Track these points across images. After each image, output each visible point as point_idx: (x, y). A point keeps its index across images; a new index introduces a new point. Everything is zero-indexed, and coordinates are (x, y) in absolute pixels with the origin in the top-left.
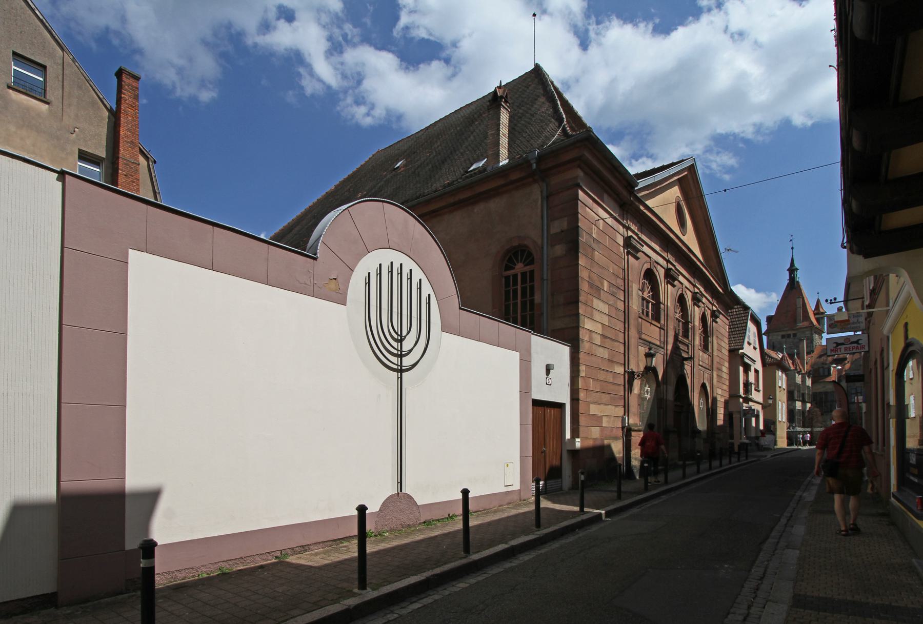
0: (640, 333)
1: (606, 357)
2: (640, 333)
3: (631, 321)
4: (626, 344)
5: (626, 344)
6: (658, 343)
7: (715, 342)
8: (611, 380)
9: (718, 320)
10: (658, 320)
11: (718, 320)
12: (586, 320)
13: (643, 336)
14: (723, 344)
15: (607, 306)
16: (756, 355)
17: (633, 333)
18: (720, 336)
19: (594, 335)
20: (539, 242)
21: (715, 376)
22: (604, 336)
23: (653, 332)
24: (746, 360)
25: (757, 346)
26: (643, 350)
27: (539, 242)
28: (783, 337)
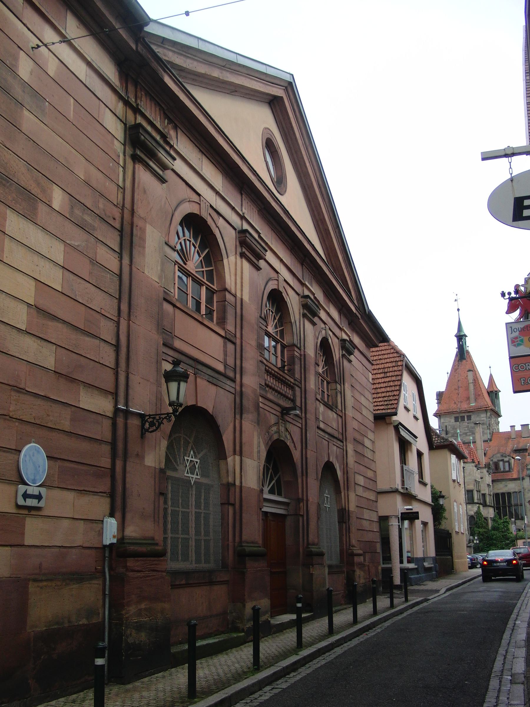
1: (50, 362)
6: (220, 367)
7: (348, 393)
8: (66, 425)
9: (352, 357)
10: (222, 322)
11: (352, 357)
14: (363, 400)
16: (418, 429)
18: (357, 386)
21: (350, 452)
24: (403, 433)
25: (419, 415)
28: (456, 419)
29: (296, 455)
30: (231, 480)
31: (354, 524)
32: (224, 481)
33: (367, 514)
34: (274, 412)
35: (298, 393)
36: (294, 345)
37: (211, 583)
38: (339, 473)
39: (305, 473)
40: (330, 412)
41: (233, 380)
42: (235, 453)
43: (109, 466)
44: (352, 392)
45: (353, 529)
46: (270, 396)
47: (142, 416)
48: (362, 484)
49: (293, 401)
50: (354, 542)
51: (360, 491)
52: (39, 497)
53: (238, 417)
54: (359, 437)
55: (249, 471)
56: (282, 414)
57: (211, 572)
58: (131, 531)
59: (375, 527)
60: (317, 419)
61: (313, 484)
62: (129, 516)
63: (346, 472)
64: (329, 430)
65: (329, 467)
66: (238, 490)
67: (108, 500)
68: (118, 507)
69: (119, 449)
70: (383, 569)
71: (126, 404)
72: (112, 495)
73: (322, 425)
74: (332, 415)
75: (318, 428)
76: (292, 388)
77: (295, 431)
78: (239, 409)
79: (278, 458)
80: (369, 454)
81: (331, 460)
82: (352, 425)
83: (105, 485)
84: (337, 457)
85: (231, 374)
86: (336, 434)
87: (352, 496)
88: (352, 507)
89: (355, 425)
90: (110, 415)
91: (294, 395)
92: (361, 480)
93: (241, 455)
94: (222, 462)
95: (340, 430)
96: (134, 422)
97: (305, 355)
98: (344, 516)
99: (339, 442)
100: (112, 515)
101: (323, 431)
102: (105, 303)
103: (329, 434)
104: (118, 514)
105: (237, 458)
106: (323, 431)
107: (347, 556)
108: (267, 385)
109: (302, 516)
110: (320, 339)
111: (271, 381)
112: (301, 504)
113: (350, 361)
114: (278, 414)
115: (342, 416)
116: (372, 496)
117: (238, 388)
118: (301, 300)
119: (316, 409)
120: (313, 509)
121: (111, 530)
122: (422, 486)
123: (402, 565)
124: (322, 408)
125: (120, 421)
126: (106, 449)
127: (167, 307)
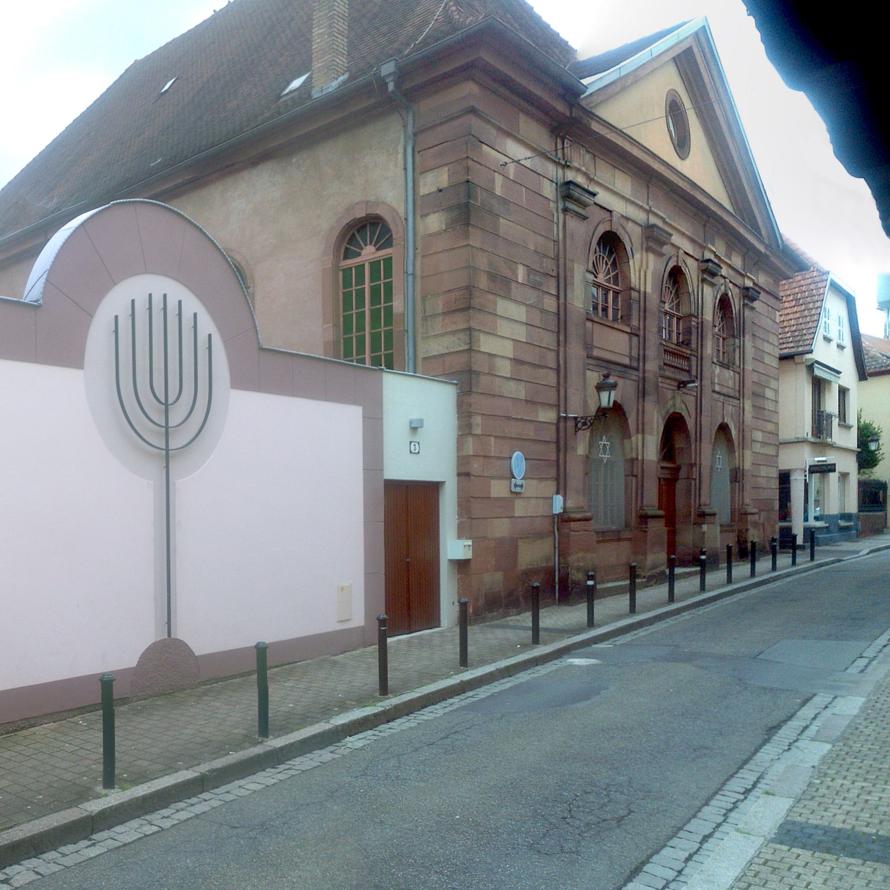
0: (588, 346)
2: (588, 346)
3: (572, 330)
4: (561, 371)
5: (561, 371)
6: (626, 361)
7: (749, 345)
12: (482, 337)
13: (596, 353)
15: (523, 309)
17: (575, 351)
19: (499, 362)
20: (401, 211)
22: (517, 361)
23: (615, 344)
26: (594, 377)
27: (401, 211)
29: (690, 423)
30: (634, 456)
31: (749, 483)
32: (628, 457)
33: (764, 471)
34: (670, 387)
35: (694, 363)
36: (691, 315)
37: (619, 540)
38: (734, 432)
39: (699, 438)
40: (726, 371)
41: (637, 369)
42: (638, 432)
43: (555, 459)
44: (754, 342)
45: (748, 487)
46: (668, 373)
47: (575, 418)
48: (760, 439)
49: (689, 372)
50: (747, 501)
51: (757, 448)
52: (521, 486)
53: (641, 400)
54: (758, 390)
55: (650, 447)
56: (679, 387)
57: (619, 532)
58: (569, 504)
59: (775, 484)
60: (713, 383)
61: (706, 447)
62: (568, 493)
63: (742, 431)
64: (725, 391)
65: (723, 428)
66: (640, 463)
67: (555, 482)
68: (561, 487)
69: (561, 445)
70: (782, 529)
71: (565, 412)
72: (557, 479)
73: (717, 388)
74: (728, 374)
75: (714, 391)
76: (688, 359)
77: (691, 400)
78: (642, 394)
79: (675, 425)
80: (770, 406)
81: (726, 421)
82: (750, 378)
83: (553, 472)
84: (732, 417)
85: (635, 364)
86: (732, 393)
87: (748, 454)
88: (747, 466)
89: (755, 377)
90: (555, 421)
91: (690, 366)
92: (758, 436)
93: (643, 432)
94: (626, 442)
95: (737, 388)
96: (571, 424)
97: (702, 322)
98: (737, 476)
99: (735, 401)
100: (558, 493)
101: (719, 393)
102: (549, 340)
103: (724, 395)
104: (562, 491)
105: (640, 436)
106: (719, 393)
107: (740, 516)
108: (665, 364)
109: (695, 479)
110: (719, 297)
111: (669, 359)
112: (694, 469)
113: (753, 309)
114: (674, 388)
115: (741, 375)
116: (771, 451)
117: (641, 375)
118: (701, 264)
119: (713, 373)
120: (705, 472)
121: (558, 504)
122: (843, 431)
123: (807, 524)
124: (718, 370)
125: (562, 424)
126: (553, 447)
127: (589, 324)
